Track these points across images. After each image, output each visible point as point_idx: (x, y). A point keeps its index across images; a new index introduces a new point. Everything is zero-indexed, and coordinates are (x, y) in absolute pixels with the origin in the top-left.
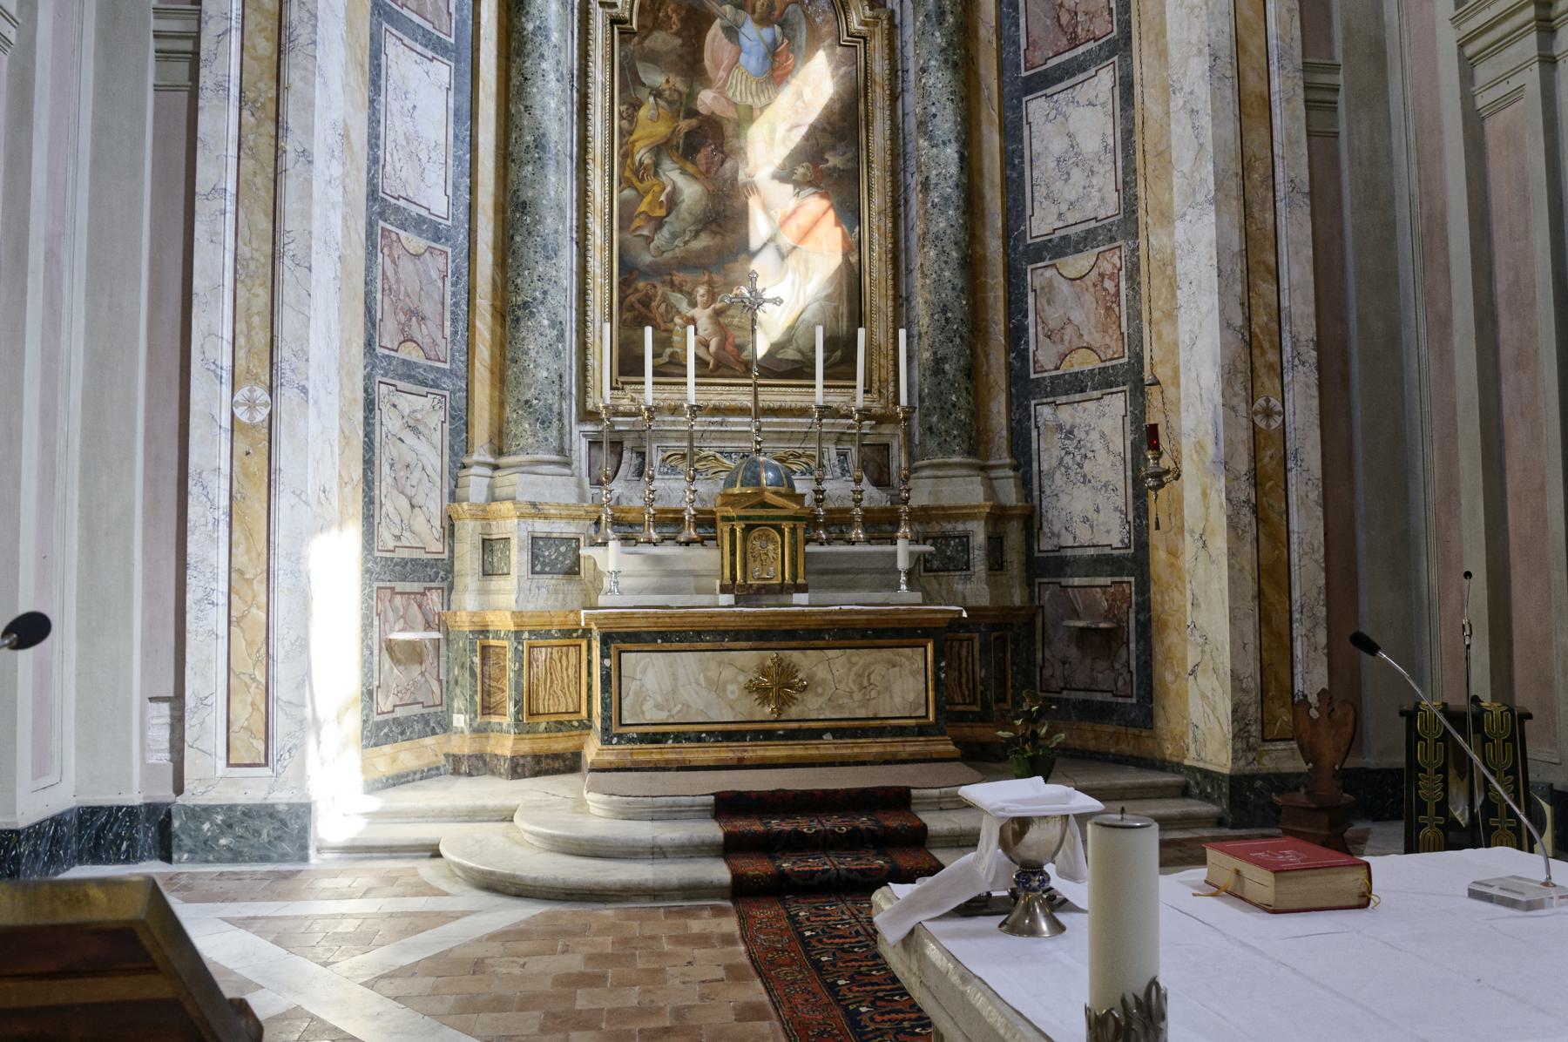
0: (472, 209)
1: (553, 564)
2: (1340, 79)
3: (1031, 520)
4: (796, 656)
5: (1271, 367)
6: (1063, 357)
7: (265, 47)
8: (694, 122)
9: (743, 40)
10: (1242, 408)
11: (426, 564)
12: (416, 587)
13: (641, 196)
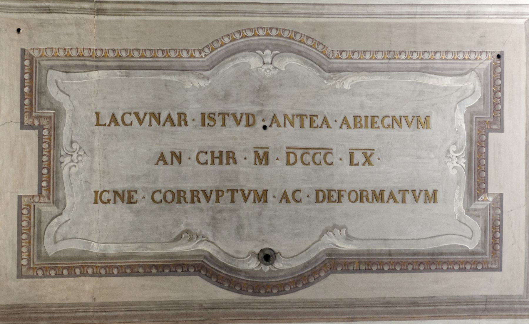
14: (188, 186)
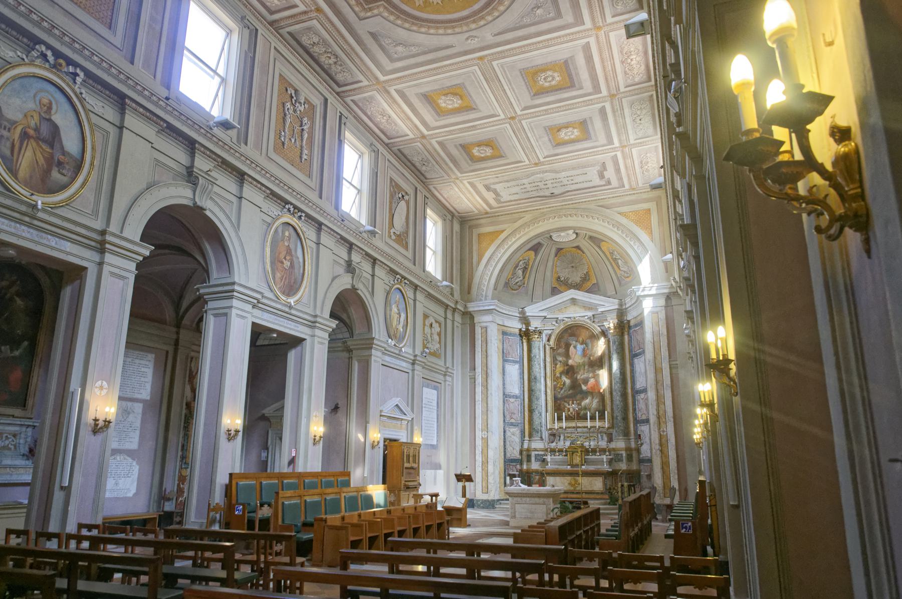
0: (524, 391)
2: (677, 362)
3: (638, 451)
5: (664, 422)
7: (485, 376)
10: (657, 430)
11: (517, 460)
12: (515, 464)
13: (558, 383)
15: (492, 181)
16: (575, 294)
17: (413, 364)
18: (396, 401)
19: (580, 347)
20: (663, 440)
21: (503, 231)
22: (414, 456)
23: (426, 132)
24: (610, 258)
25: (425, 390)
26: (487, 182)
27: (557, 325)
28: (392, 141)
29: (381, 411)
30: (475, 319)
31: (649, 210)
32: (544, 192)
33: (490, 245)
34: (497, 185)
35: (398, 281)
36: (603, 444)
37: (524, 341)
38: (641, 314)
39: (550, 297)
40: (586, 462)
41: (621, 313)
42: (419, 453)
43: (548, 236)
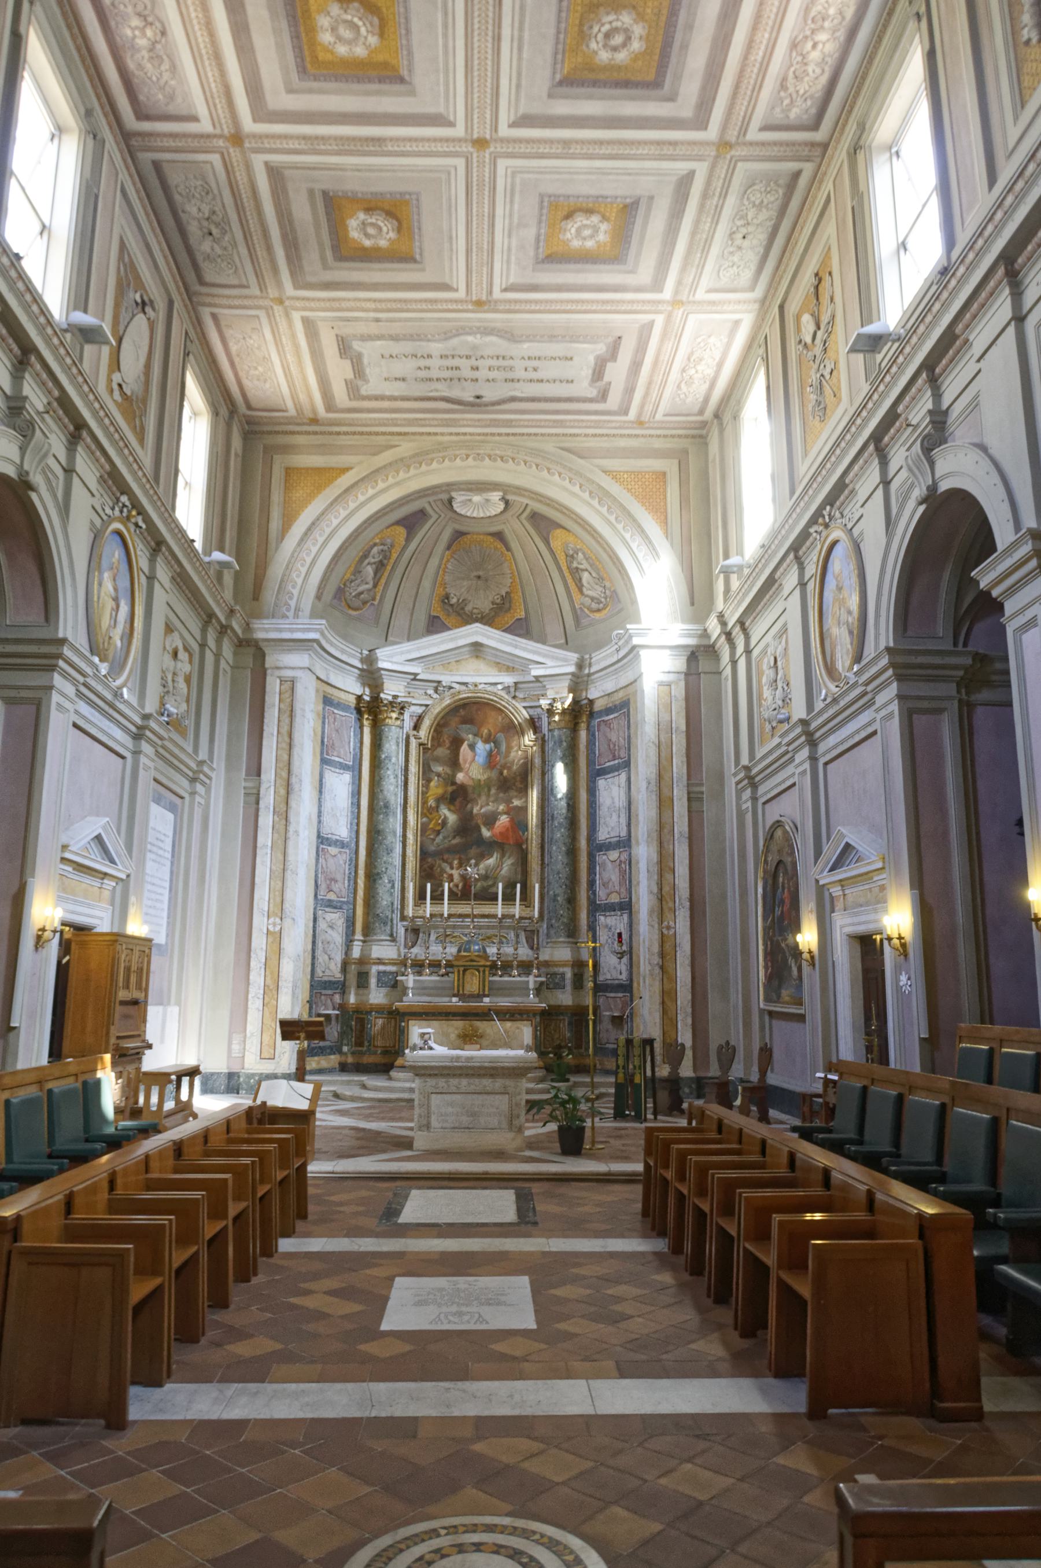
0: (357, 832)
1: (386, 983)
2: (704, 789)
4: (478, 1024)
5: (670, 909)
6: (608, 895)
7: (283, 792)
8: (454, 787)
9: (477, 750)
10: (656, 926)
11: (334, 983)
12: (330, 992)
13: (431, 820)
14: (435, 377)
15: (361, 328)
16: (484, 635)
17: (137, 737)
18: (96, 825)
19: (482, 748)
20: (668, 946)
21: (345, 470)
22: (140, 970)
23: (248, 125)
24: (564, 568)
25: (155, 809)
26: (347, 330)
27: (435, 696)
28: (146, 126)
29: (65, 847)
30: (267, 658)
31: (664, 474)
32: (463, 389)
33: (310, 497)
34: (369, 344)
35: (121, 512)
36: (524, 952)
37: (366, 723)
38: (635, 681)
39: (423, 636)
40: (495, 990)
41: (578, 682)
42: (149, 963)
43: (444, 497)
